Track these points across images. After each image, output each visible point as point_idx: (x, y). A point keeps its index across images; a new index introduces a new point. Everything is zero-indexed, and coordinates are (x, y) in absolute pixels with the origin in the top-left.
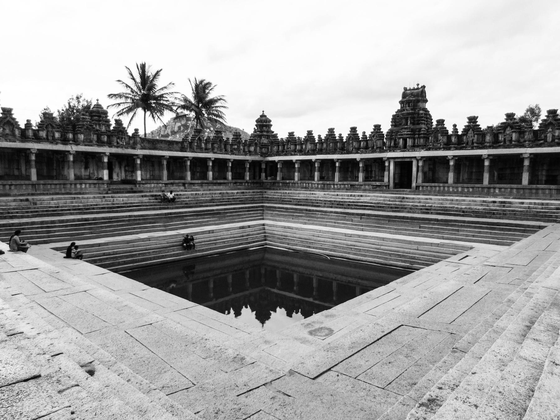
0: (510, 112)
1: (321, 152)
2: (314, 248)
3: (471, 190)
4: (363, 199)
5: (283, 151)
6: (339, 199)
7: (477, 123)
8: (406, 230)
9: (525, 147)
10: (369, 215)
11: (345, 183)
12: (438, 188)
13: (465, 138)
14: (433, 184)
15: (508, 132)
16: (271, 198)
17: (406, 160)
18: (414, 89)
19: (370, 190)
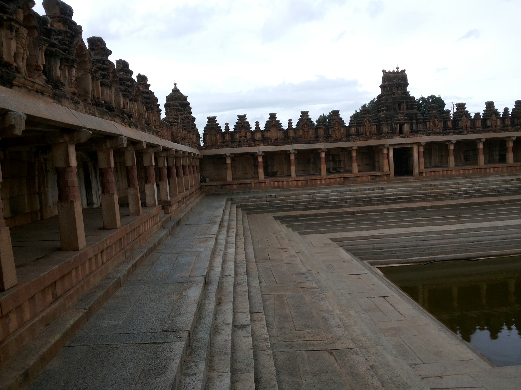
0: (490, 100)
1: (296, 141)
2: (438, 254)
3: (471, 171)
4: (388, 192)
5: (232, 142)
6: (358, 195)
7: (466, 110)
8: (488, 216)
9: (509, 131)
10: (432, 207)
11: (337, 175)
12: (441, 173)
13: (460, 123)
14: (438, 169)
15: (494, 118)
16: (251, 206)
17: (406, 146)
18: (394, 72)
19: (369, 182)
